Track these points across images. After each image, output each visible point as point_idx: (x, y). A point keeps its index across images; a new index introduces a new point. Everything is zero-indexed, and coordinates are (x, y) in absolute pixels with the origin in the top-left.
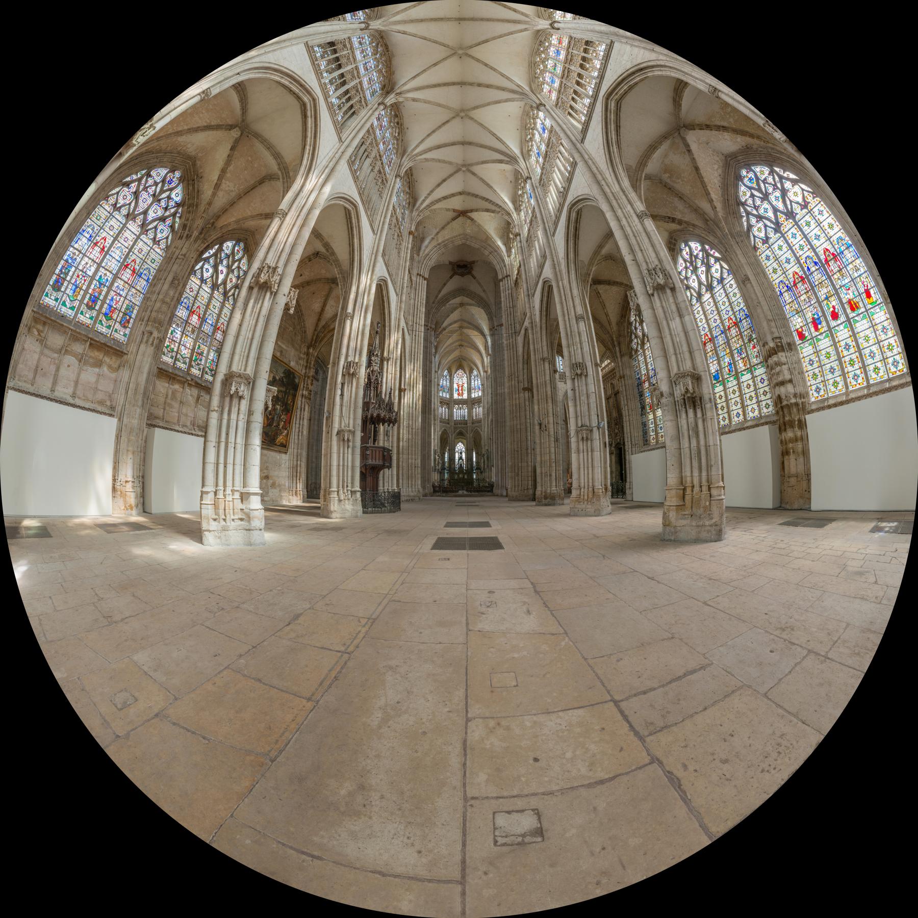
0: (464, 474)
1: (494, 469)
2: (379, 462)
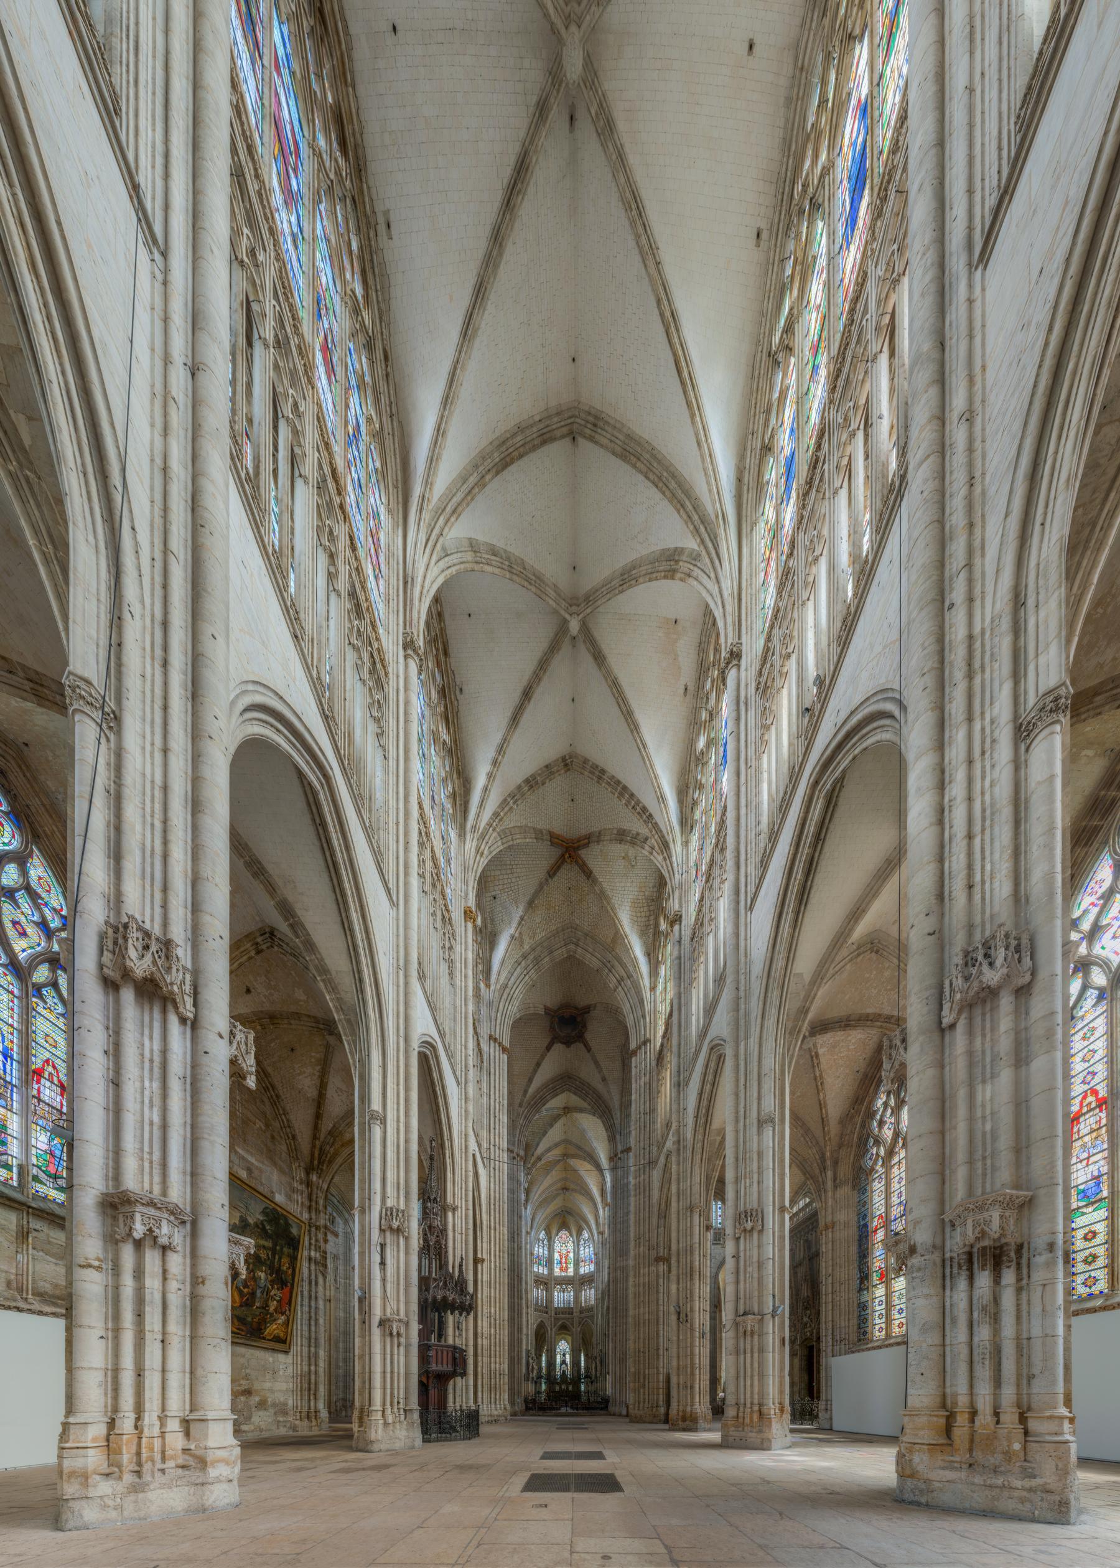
0: (568, 1384)
1: (609, 1378)
2: (447, 1368)
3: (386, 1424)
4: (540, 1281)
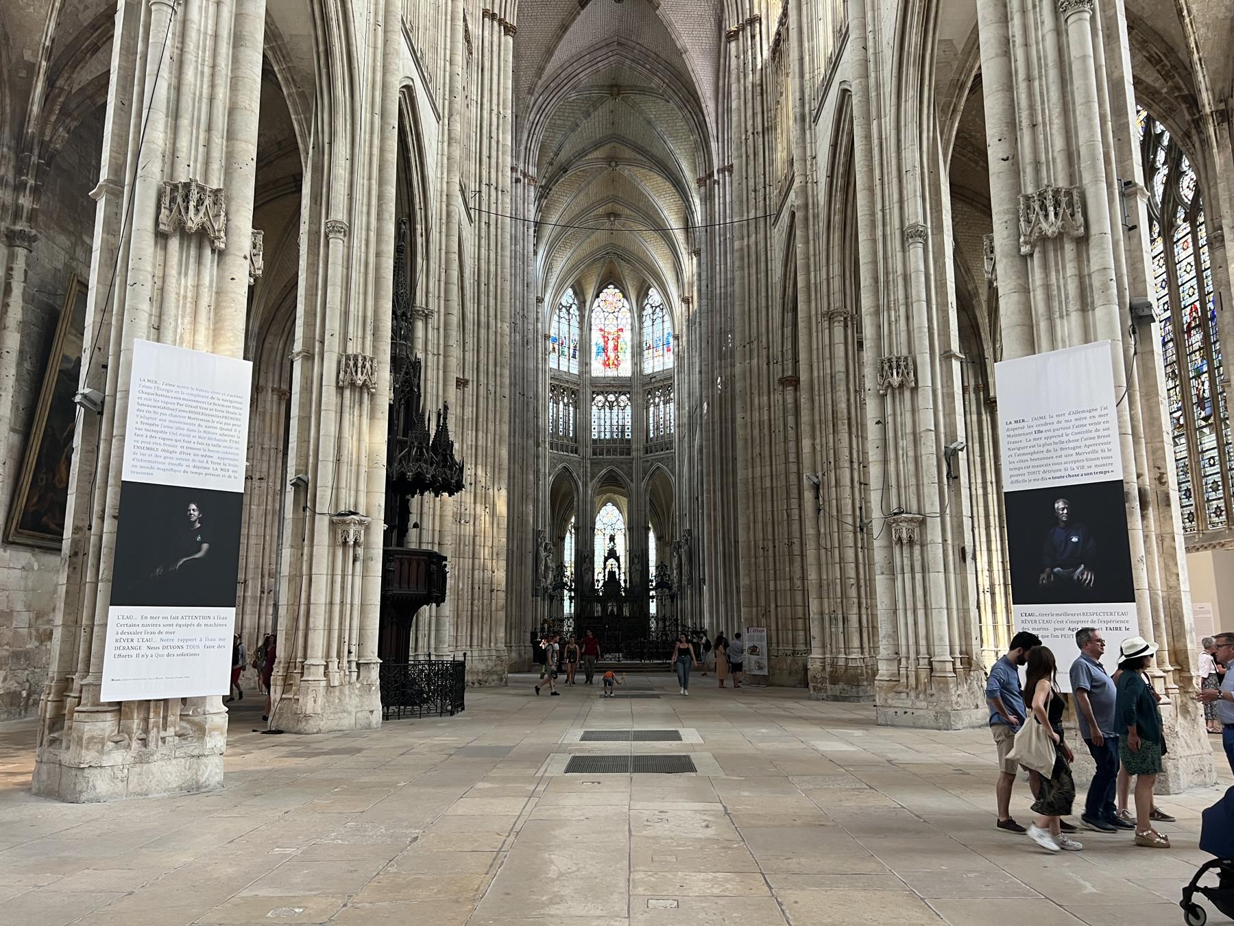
0: (620, 601)
3: (329, 687)
4: (564, 388)
